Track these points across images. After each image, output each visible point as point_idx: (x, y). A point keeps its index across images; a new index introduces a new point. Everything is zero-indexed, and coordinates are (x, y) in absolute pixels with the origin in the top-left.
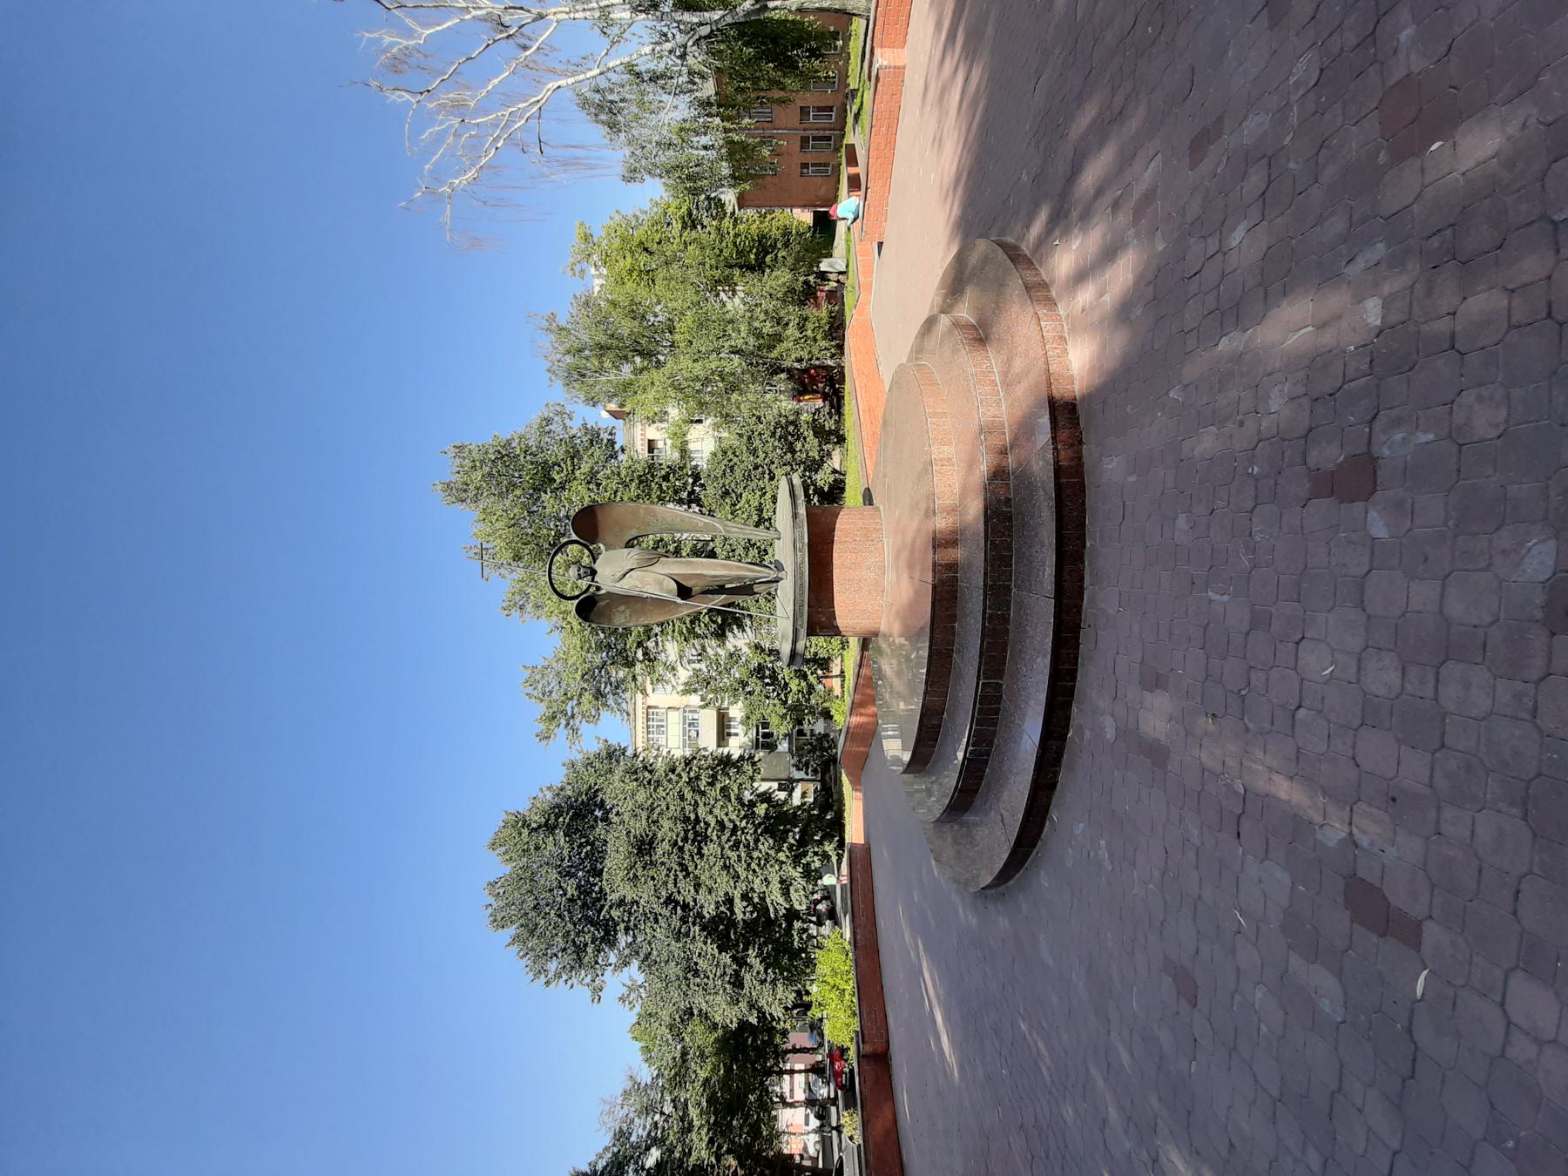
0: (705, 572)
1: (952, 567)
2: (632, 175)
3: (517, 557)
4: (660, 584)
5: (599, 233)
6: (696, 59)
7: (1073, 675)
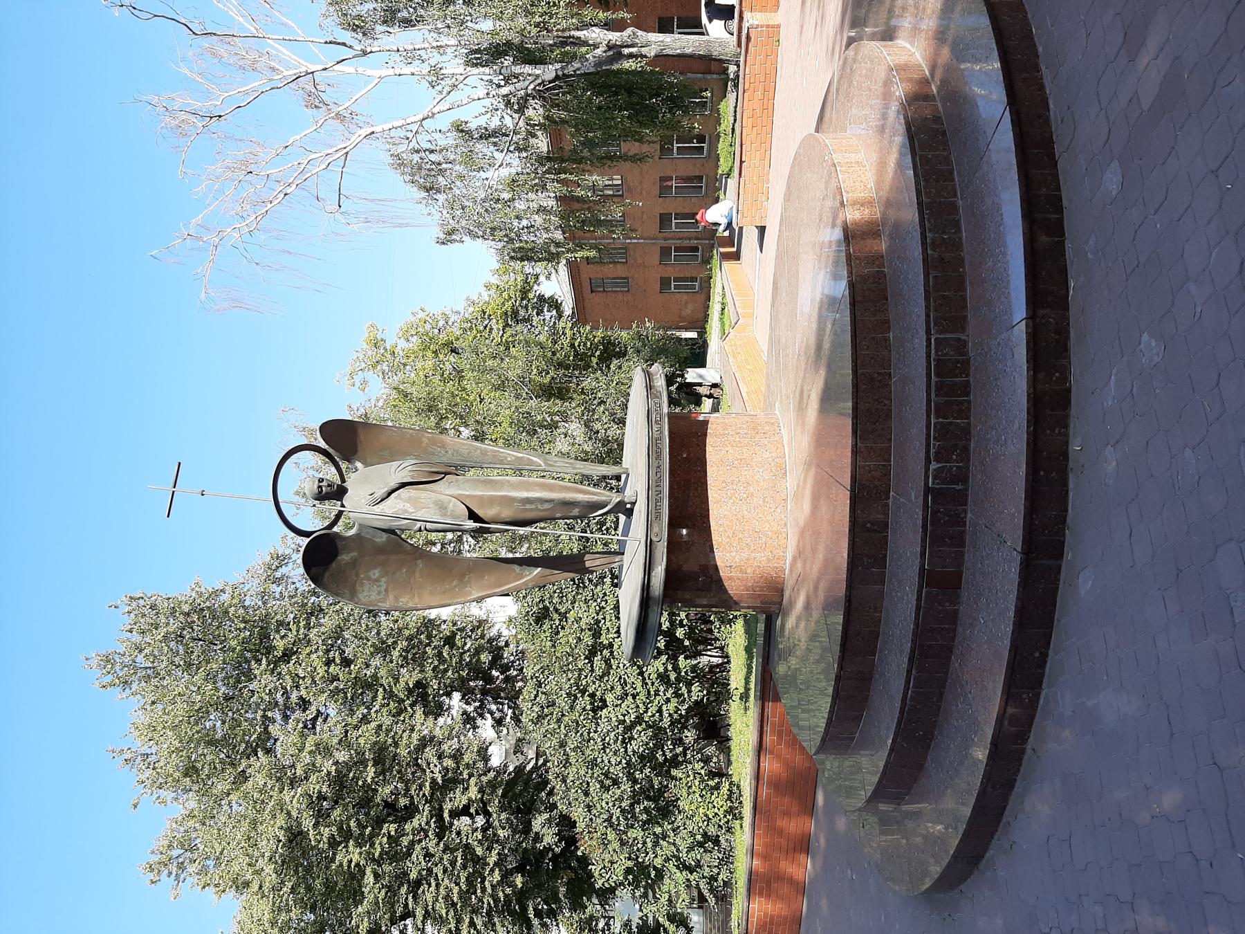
0: (513, 494)
1: (877, 259)
2: (449, 237)
3: (191, 770)
4: (442, 507)
5: (392, 338)
6: (536, 112)
7: (1057, 205)
